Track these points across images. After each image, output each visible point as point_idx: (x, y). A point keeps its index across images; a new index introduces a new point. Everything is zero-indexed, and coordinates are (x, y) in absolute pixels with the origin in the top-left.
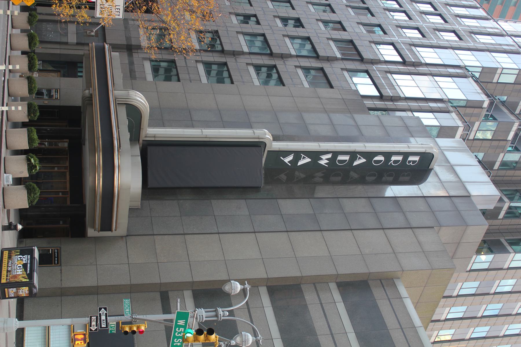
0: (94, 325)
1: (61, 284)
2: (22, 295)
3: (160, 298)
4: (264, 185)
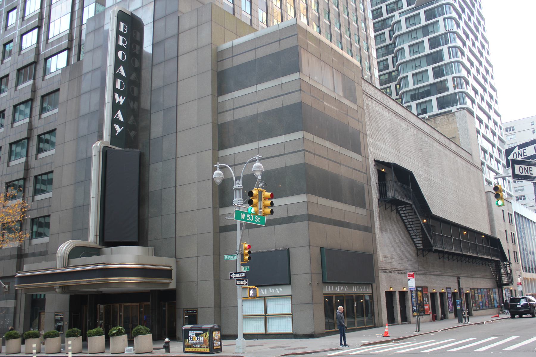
0: (243, 282)
1: (212, 307)
3: (225, 233)
4: (138, 149)
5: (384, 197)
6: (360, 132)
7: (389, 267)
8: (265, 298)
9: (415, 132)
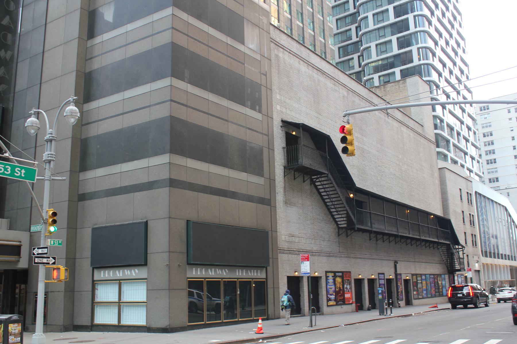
0: (47, 260)
2: (19, 330)
3: (83, 202)
4: (1, 104)
5: (291, 164)
6: (262, 86)
7: (295, 247)
8: (120, 282)
9: (345, 93)
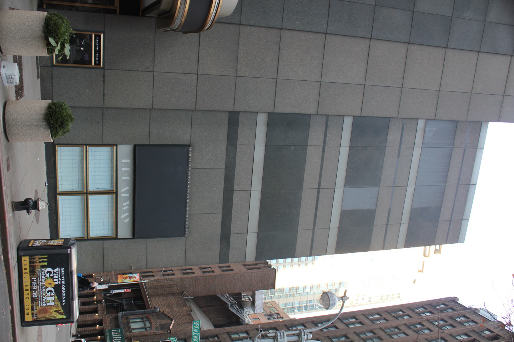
1: (104, 102)
8: (114, 193)
